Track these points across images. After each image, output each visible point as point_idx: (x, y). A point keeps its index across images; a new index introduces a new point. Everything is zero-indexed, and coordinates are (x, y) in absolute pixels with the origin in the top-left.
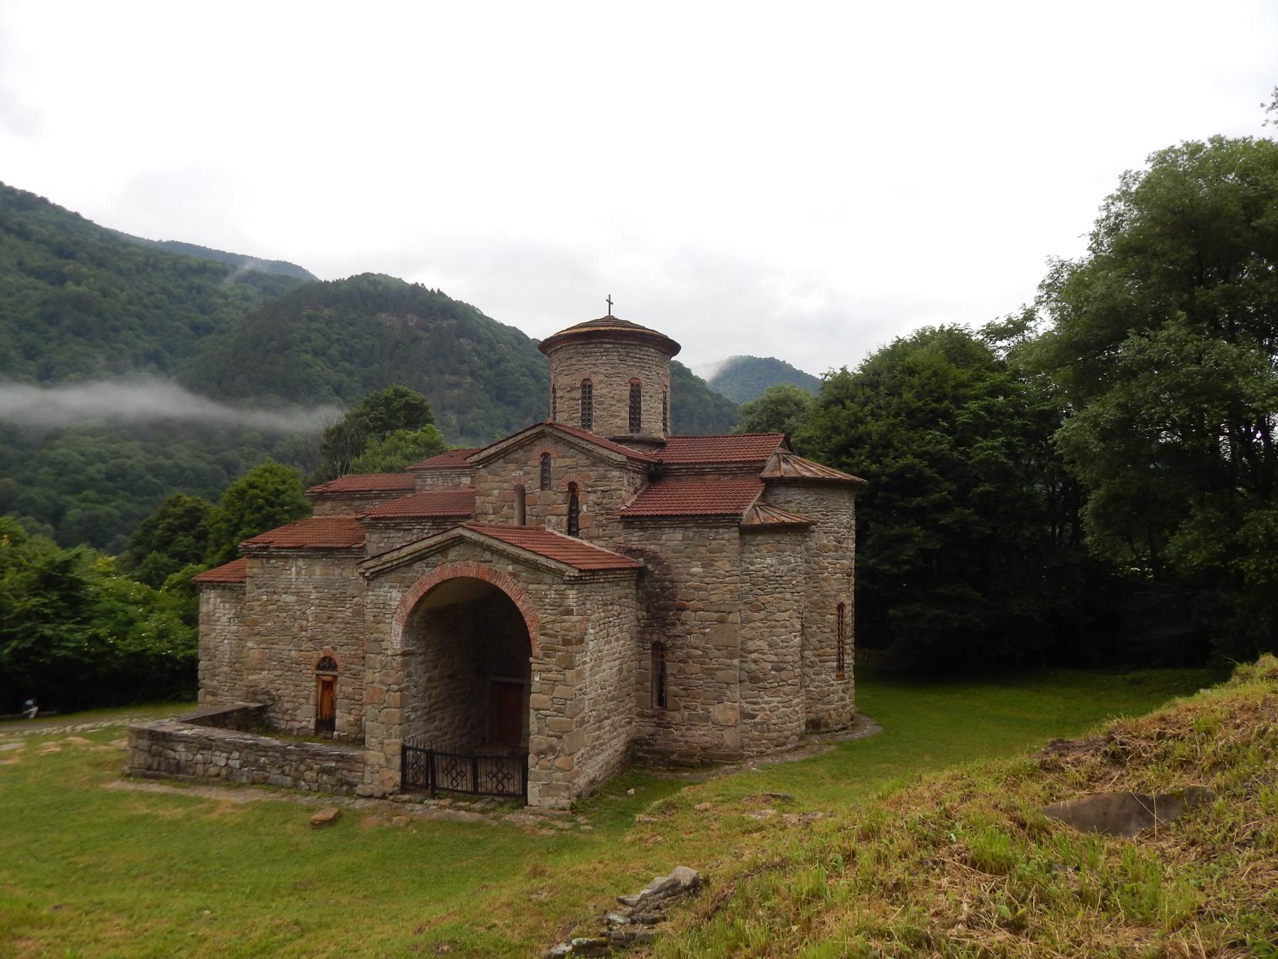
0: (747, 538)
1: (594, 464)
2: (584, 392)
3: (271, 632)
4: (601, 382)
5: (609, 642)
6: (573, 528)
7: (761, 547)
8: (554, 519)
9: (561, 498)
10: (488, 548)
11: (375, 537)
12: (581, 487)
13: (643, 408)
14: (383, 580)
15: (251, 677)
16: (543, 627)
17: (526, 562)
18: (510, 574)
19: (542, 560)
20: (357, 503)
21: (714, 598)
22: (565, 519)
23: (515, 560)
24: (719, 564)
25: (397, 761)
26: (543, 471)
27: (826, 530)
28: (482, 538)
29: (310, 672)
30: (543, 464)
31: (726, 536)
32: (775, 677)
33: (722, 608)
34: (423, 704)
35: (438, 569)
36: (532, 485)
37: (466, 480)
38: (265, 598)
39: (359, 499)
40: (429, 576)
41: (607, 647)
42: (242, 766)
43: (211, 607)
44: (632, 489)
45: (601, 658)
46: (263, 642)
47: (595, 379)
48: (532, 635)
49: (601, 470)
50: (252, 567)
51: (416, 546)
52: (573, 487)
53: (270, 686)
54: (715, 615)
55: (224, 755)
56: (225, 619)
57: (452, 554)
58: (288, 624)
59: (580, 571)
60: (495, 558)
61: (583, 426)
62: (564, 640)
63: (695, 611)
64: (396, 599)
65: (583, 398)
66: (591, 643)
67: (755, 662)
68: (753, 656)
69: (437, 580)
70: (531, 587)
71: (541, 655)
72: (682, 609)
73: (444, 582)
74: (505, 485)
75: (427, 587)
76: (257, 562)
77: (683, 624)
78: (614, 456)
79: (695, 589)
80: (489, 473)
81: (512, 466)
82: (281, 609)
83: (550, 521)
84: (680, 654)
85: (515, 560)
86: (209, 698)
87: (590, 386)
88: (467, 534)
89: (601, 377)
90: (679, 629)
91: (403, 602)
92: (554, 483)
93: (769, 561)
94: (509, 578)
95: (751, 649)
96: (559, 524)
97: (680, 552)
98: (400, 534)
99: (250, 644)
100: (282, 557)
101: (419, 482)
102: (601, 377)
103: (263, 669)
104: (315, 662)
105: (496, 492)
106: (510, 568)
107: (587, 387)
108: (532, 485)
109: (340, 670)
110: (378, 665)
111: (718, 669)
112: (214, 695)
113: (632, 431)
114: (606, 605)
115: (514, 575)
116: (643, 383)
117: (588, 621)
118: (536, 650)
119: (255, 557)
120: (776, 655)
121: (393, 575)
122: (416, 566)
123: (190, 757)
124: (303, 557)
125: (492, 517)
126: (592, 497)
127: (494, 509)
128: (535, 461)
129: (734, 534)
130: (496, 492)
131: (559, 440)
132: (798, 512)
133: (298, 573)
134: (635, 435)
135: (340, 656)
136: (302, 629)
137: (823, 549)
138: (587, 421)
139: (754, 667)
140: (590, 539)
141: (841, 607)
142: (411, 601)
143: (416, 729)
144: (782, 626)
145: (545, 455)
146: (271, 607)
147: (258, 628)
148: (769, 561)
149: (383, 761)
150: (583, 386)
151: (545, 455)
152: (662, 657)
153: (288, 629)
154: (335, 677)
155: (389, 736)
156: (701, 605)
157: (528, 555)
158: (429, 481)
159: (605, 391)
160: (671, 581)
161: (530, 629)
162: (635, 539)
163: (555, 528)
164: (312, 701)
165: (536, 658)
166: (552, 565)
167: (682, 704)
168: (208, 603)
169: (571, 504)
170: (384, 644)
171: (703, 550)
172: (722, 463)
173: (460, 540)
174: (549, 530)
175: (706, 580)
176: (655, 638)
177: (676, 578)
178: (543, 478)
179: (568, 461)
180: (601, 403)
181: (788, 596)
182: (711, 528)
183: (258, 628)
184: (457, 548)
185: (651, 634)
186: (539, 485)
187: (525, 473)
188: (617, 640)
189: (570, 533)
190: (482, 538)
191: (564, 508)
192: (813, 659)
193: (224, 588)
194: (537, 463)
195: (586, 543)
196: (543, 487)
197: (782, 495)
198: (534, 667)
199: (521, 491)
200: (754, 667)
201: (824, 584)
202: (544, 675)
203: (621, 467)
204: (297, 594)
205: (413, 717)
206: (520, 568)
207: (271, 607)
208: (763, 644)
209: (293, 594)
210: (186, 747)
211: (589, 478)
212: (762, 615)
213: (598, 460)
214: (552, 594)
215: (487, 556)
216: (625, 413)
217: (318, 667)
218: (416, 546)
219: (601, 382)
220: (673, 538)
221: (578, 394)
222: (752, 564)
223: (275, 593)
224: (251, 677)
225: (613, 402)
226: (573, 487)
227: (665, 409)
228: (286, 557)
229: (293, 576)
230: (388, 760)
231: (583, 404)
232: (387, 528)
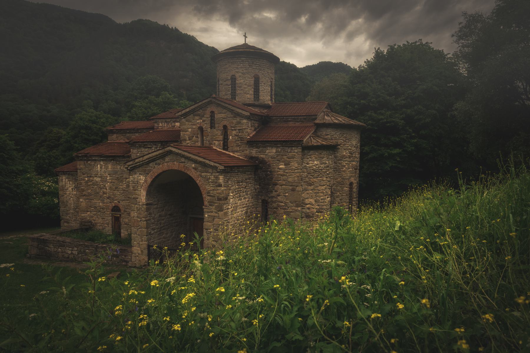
0: (306, 151)
1: (235, 117)
2: (232, 82)
3: (90, 195)
4: (240, 76)
5: (241, 200)
6: (225, 146)
8: (217, 143)
9: (219, 133)
10: (183, 156)
11: (135, 151)
12: (229, 127)
13: (260, 90)
14: (136, 171)
15: (83, 215)
16: (208, 192)
17: (200, 163)
18: (193, 168)
19: (207, 162)
20: (128, 135)
21: (290, 180)
22: (222, 143)
23: (195, 162)
24: (292, 164)
25: (146, 252)
26: (211, 120)
28: (180, 152)
29: (109, 212)
30: (211, 116)
31: (296, 151)
33: (294, 184)
34: (157, 227)
35: (161, 166)
36: (206, 126)
37: (177, 124)
38: (87, 179)
39: (129, 133)
40: (157, 169)
41: (240, 201)
42: (78, 254)
43: (64, 183)
44: (253, 129)
45: (237, 207)
46: (87, 199)
47: (237, 75)
48: (204, 196)
49: (238, 119)
50: (80, 165)
51: (150, 155)
52: (225, 127)
53: (91, 219)
54: (291, 187)
55: (70, 249)
56: (70, 189)
57: (167, 159)
58: (98, 191)
59: (225, 167)
60: (186, 161)
61: (232, 98)
62: (218, 198)
63: (281, 186)
64: (142, 179)
65: (231, 84)
66: (231, 200)
67: (309, 209)
68: (308, 206)
69: (161, 171)
70: (203, 174)
71: (208, 205)
72: (276, 184)
73: (164, 172)
74: (194, 127)
75: (156, 174)
76: (82, 162)
77: (276, 191)
78: (244, 113)
79: (281, 175)
80: (186, 121)
81: (197, 118)
82: (94, 184)
83: (215, 144)
84: (275, 205)
85: (195, 162)
86: (66, 224)
87: (235, 79)
88: (174, 150)
89: (240, 74)
90: (274, 194)
91: (146, 181)
92: (216, 125)
93: (316, 162)
94: (193, 170)
95: (307, 203)
96: (219, 145)
97: (274, 158)
98: (147, 150)
99: (81, 200)
100: (93, 160)
101: (156, 125)
102: (240, 74)
103: (88, 211)
104: (111, 208)
105: (190, 130)
106: (193, 165)
107: (233, 79)
108: (206, 126)
109: (122, 212)
110: (136, 209)
111: (291, 212)
112: (68, 223)
113: (255, 101)
114: (239, 182)
115: (195, 169)
116: (260, 77)
117: (230, 189)
118: (206, 203)
119: (81, 160)
120: (318, 205)
121: (141, 169)
122: (151, 165)
123: (56, 250)
124: (103, 160)
125: (188, 141)
126: (234, 132)
127: (189, 138)
128: (208, 115)
129: (299, 150)
130: (190, 130)
131: (218, 105)
132: (332, 139)
133: (101, 168)
134: (256, 103)
135: (122, 204)
136: (104, 193)
137: (344, 157)
138: (234, 95)
139: (308, 211)
140: (233, 152)
141: (351, 184)
142: (149, 180)
143: (154, 238)
144: (321, 193)
145: (212, 112)
146: (89, 183)
147: (84, 193)
148: (316, 162)
149: (140, 252)
150: (232, 78)
151: (212, 112)
152: (267, 206)
153: (98, 193)
154: (120, 215)
155: (142, 241)
156: (284, 183)
157: (201, 159)
158: (160, 125)
159: (242, 81)
160: (271, 172)
161: (203, 193)
162: (254, 152)
163: (217, 147)
164: (110, 226)
165: (206, 206)
166: (212, 164)
168: (62, 181)
169: (225, 136)
170: (138, 200)
171: (285, 157)
172: (296, 116)
173: (171, 152)
174: (215, 148)
175: (286, 171)
176: (263, 198)
177: (273, 170)
178: (211, 123)
179: (223, 115)
180: (240, 87)
181: (325, 179)
182: (289, 147)
183: (84, 193)
184: (169, 156)
185: (262, 196)
186: (209, 127)
187: (203, 121)
188: (245, 198)
189: (224, 149)
190: (180, 152)
191: (221, 138)
193: (69, 174)
194: (208, 116)
195: (231, 154)
196: (212, 126)
197: (324, 132)
198: (205, 210)
199: (201, 129)
200: (308, 211)
201: (343, 173)
202: (209, 214)
203: (248, 118)
204: (101, 177)
205: (152, 232)
206: (197, 165)
207: (89, 183)
208: (312, 201)
209: (99, 177)
210: (53, 245)
211: (233, 123)
212: (312, 187)
213: (237, 115)
214: (212, 177)
215: (183, 160)
216: (252, 92)
217: (112, 210)
218: (150, 155)
219: (240, 76)
220: (272, 152)
221: (229, 82)
222: (308, 164)
223: (91, 177)
224: (83, 215)
225: (245, 86)
226: (225, 127)
227: (271, 89)
228: (95, 160)
229: (99, 169)
230: (142, 251)
231: (232, 87)
232: (140, 147)
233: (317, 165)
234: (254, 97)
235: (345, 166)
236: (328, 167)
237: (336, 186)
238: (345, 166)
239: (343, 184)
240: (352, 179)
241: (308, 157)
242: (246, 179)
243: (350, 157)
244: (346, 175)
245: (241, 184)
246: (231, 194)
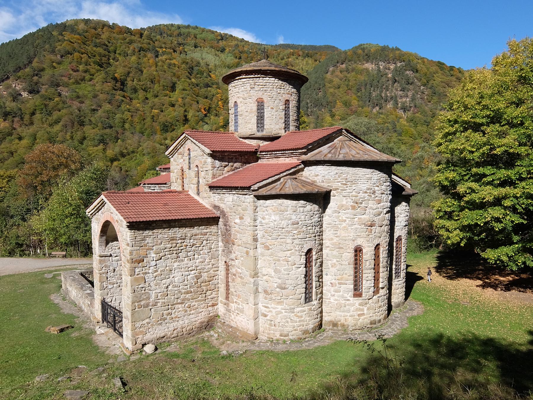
7: (268, 209)
27: (345, 194)
32: (278, 293)
36: (186, 167)
47: (238, 102)
77: (234, 253)
81: (180, 156)
89: (241, 99)
93: (273, 218)
108: (186, 167)
113: (258, 131)
132: (323, 182)
134: (259, 134)
148: (273, 218)
167: (235, 300)
175: (241, 227)
191: (195, 180)
192: (333, 281)
195: (201, 201)
196: (189, 168)
216: (254, 120)
233: (275, 221)
234: (258, 127)
235: (345, 221)
236: (293, 224)
237: (331, 250)
238: (345, 221)
239: (342, 248)
240: (359, 242)
241: (264, 209)
242: (195, 235)
243: (353, 208)
244: (346, 235)
245: (180, 241)
246: (153, 255)
